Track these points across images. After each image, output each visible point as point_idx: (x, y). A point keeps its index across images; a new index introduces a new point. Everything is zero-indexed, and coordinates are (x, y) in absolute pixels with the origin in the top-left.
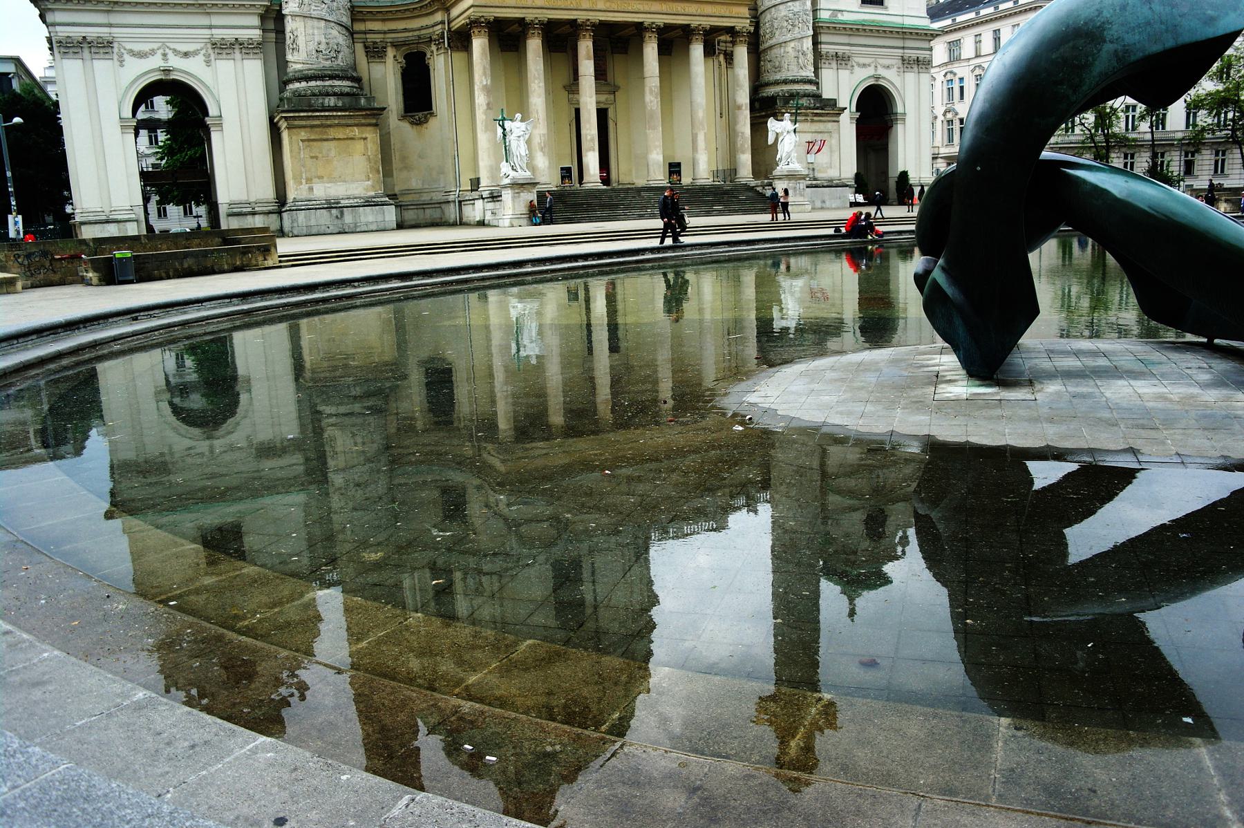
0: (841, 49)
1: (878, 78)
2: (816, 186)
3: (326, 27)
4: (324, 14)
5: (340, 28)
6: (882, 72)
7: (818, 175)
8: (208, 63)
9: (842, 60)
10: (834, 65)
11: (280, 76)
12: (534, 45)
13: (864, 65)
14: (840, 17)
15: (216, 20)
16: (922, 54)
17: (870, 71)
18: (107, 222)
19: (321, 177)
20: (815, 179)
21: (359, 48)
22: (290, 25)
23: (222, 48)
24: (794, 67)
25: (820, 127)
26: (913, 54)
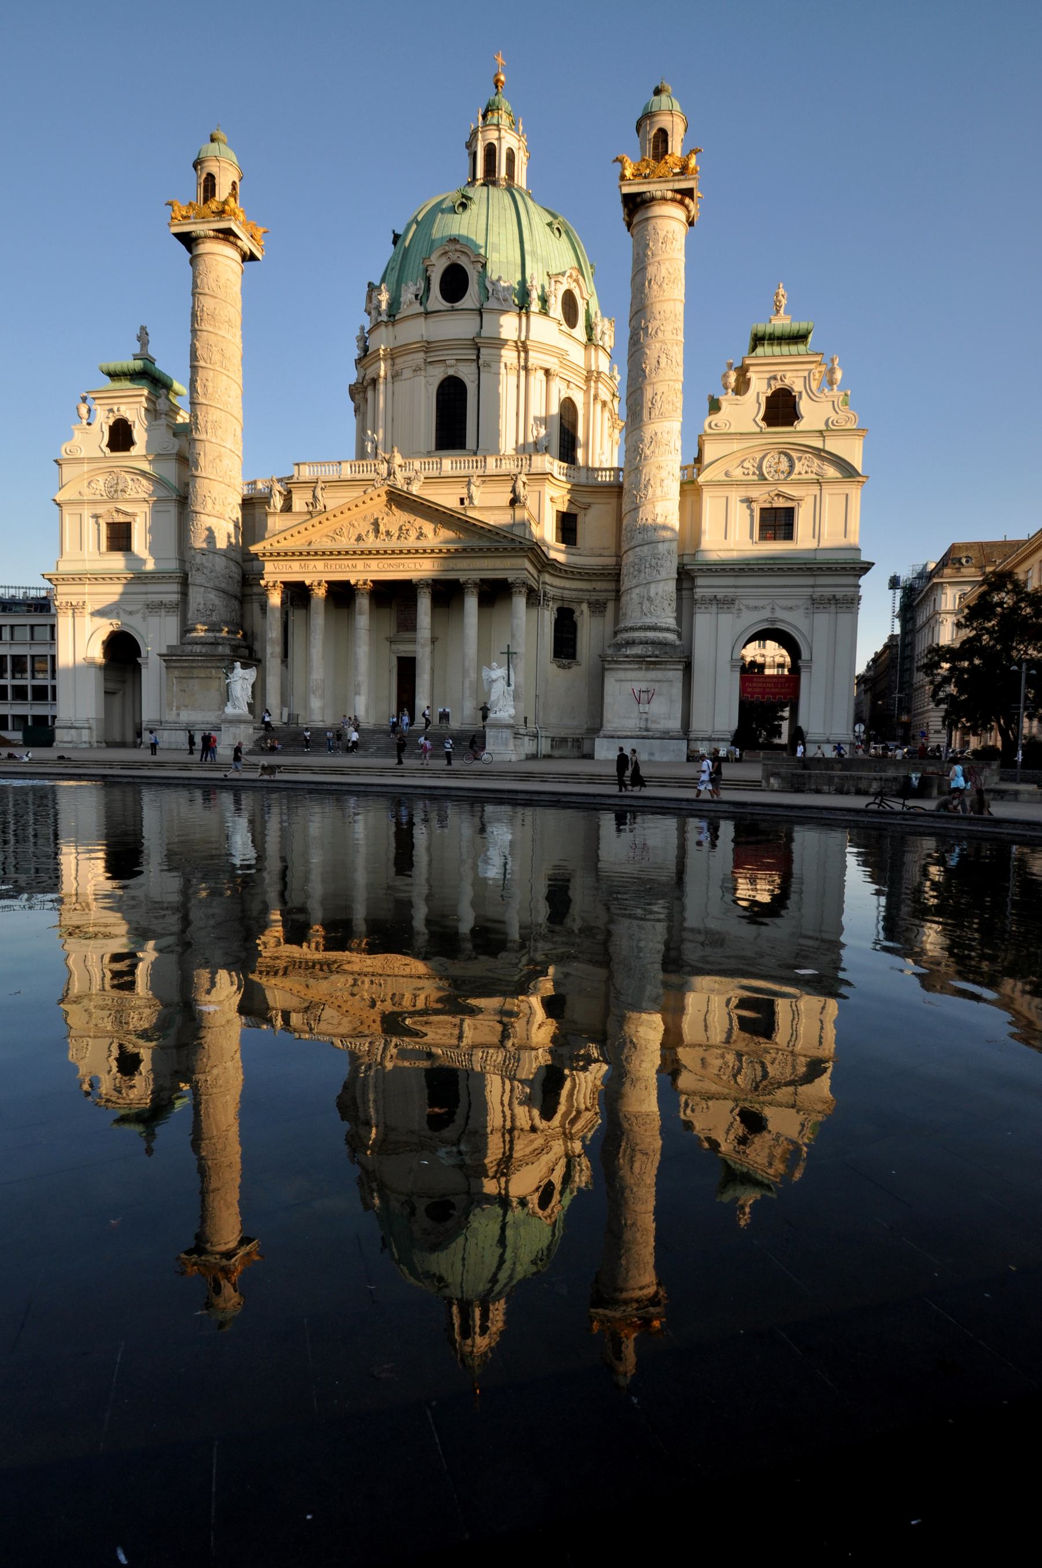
0: (720, 593)
1: (773, 621)
2: (643, 738)
3: (205, 592)
4: (204, 582)
5: (216, 593)
6: (780, 614)
7: (650, 725)
8: (144, 618)
9: (725, 603)
10: (714, 608)
11: (186, 629)
15: (151, 588)
16: (840, 592)
17: (766, 614)
18: (70, 728)
19: (186, 706)
20: (647, 730)
22: (191, 590)
23: (155, 607)
24: (637, 614)
26: (828, 592)
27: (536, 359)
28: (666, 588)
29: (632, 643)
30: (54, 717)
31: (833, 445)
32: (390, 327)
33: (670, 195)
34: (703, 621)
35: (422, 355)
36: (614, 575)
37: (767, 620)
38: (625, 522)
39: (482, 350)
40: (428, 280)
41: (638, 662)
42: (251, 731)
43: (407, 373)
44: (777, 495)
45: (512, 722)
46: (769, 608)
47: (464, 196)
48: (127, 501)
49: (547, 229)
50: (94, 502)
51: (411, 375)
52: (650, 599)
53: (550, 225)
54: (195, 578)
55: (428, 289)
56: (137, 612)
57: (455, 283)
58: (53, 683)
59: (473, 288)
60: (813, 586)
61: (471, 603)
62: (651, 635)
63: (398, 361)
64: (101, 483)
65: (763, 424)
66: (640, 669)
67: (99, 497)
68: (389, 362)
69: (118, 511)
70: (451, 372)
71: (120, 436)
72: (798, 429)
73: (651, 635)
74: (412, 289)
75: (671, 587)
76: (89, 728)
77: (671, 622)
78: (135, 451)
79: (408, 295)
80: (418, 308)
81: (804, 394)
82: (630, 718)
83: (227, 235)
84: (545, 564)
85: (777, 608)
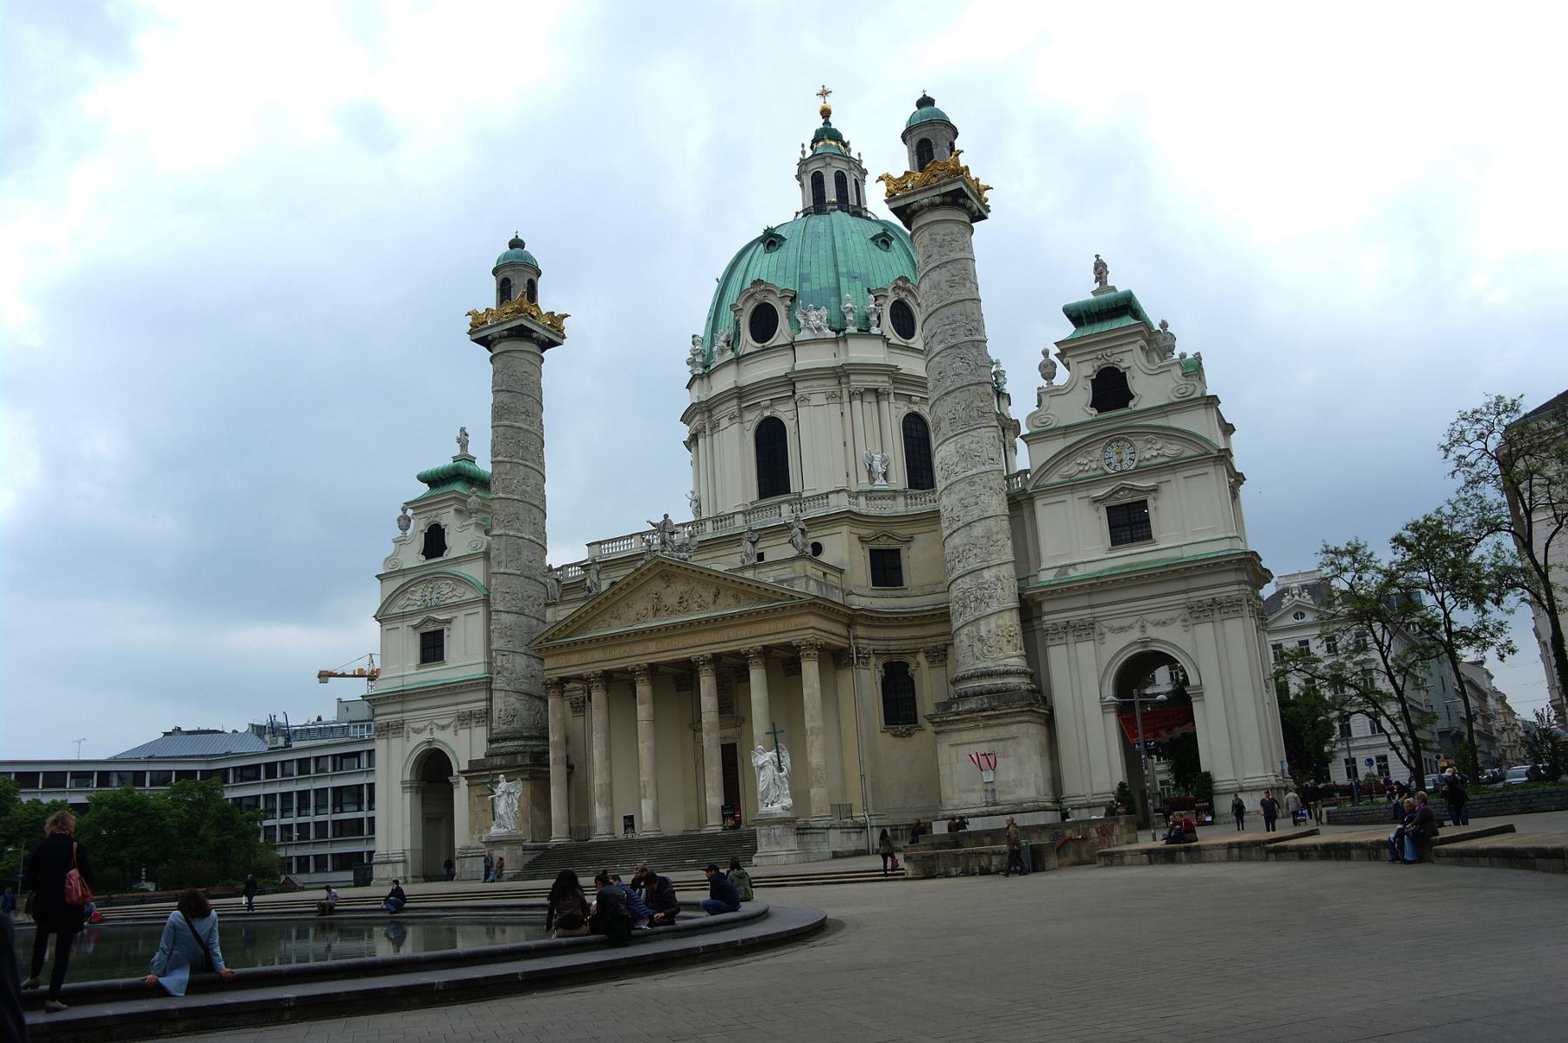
0: (1074, 616)
1: (1144, 643)
2: (990, 814)
6: (1153, 632)
7: (1001, 798)
9: (1085, 630)
10: (1071, 639)
13: (1122, 629)
14: (1072, 573)
15: (461, 698)
17: (1135, 635)
20: (995, 804)
21: (567, 703)
23: (466, 719)
24: (970, 660)
25: (1001, 732)
26: (1205, 596)
28: (1001, 622)
29: (964, 696)
30: (371, 853)
31: (1178, 421)
33: (938, 200)
34: (1057, 657)
35: (735, 402)
36: (941, 615)
37: (1135, 643)
40: (737, 323)
41: (975, 720)
42: (520, 852)
43: (724, 423)
44: (1123, 489)
45: (788, 815)
46: (1137, 627)
48: (438, 608)
49: (872, 245)
50: (412, 614)
52: (981, 639)
53: (873, 239)
54: (499, 683)
55: (737, 335)
56: (449, 726)
57: (764, 322)
58: (371, 814)
61: (757, 677)
62: (986, 683)
64: (418, 596)
65: (1095, 412)
66: (977, 727)
70: (767, 413)
71: (435, 542)
72: (1138, 408)
73: (986, 683)
75: (1011, 621)
76: (405, 862)
77: (1016, 662)
78: (450, 554)
81: (1134, 367)
82: (972, 791)
83: (522, 333)
84: (852, 618)
85: (1149, 626)
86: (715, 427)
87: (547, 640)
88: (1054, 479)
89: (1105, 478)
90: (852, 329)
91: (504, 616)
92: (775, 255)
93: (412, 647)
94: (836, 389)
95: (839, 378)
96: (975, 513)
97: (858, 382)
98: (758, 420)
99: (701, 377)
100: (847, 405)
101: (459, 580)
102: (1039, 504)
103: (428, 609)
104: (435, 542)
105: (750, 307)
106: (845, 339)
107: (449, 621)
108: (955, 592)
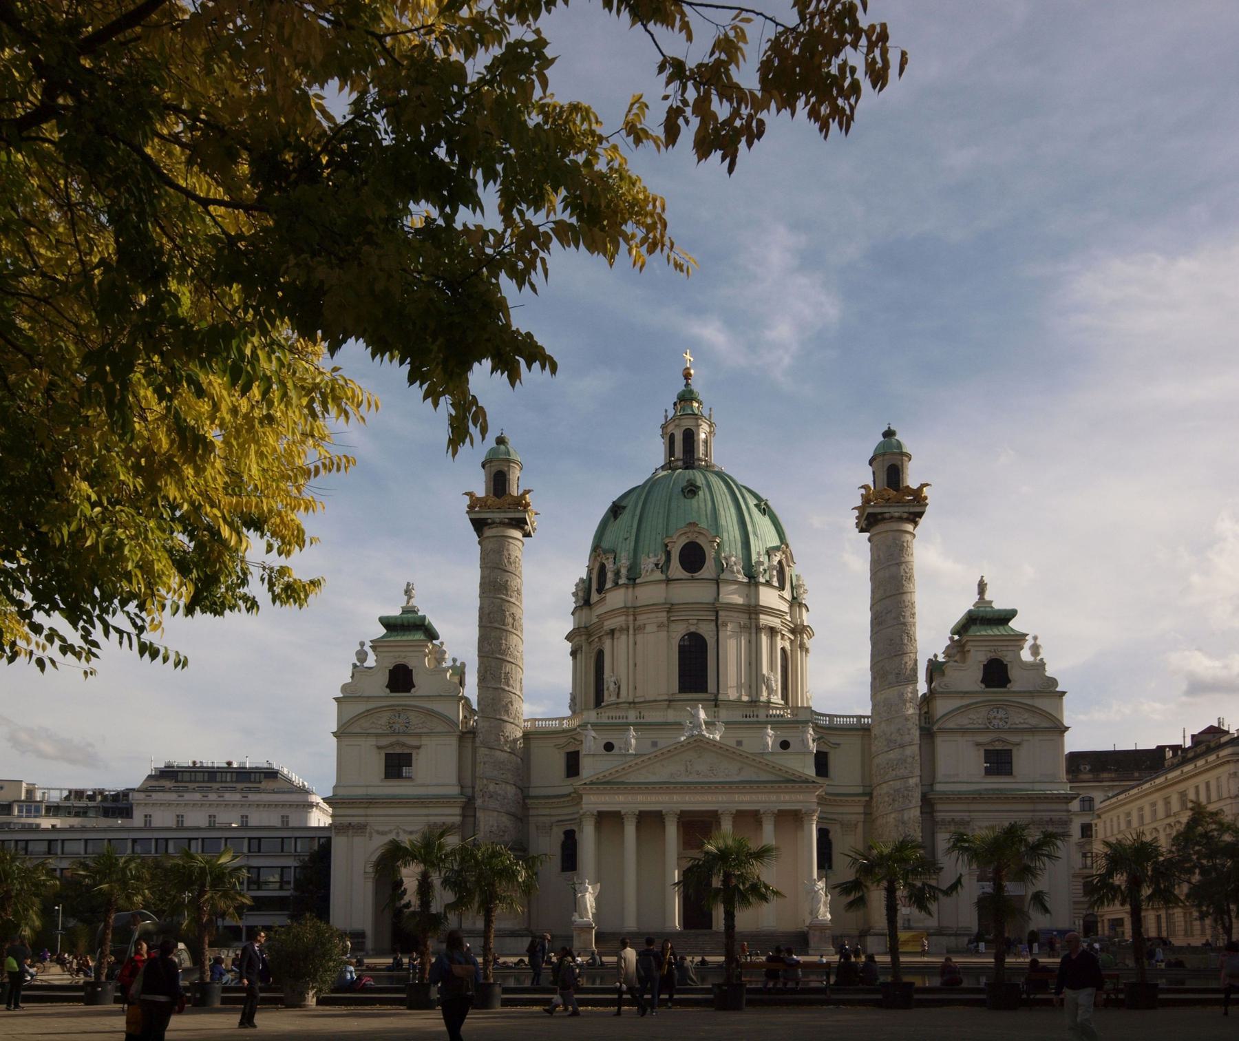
12: (630, 829)
27: (765, 620)
32: (630, 590)
35: (665, 614)
38: (876, 761)
39: (720, 613)
40: (668, 554)
43: (649, 628)
47: (692, 485)
48: (410, 735)
50: (377, 735)
51: (655, 629)
57: (693, 558)
59: (710, 563)
60: (1034, 811)
63: (639, 617)
64: (383, 721)
67: (380, 731)
68: (631, 618)
69: (398, 743)
70: (693, 629)
71: (401, 679)
74: (653, 560)
79: (648, 563)
80: (658, 575)
86: (638, 629)
87: (592, 783)
88: (951, 725)
89: (986, 730)
90: (762, 580)
91: (498, 753)
92: (694, 501)
93: (377, 764)
94: (747, 621)
95: (750, 614)
96: (907, 738)
97: (765, 620)
98: (684, 632)
99: (626, 586)
100: (754, 635)
101: (431, 713)
102: (939, 740)
103: (394, 733)
104: (401, 679)
105: (683, 541)
106: (757, 584)
107: (418, 747)
108: (885, 788)
